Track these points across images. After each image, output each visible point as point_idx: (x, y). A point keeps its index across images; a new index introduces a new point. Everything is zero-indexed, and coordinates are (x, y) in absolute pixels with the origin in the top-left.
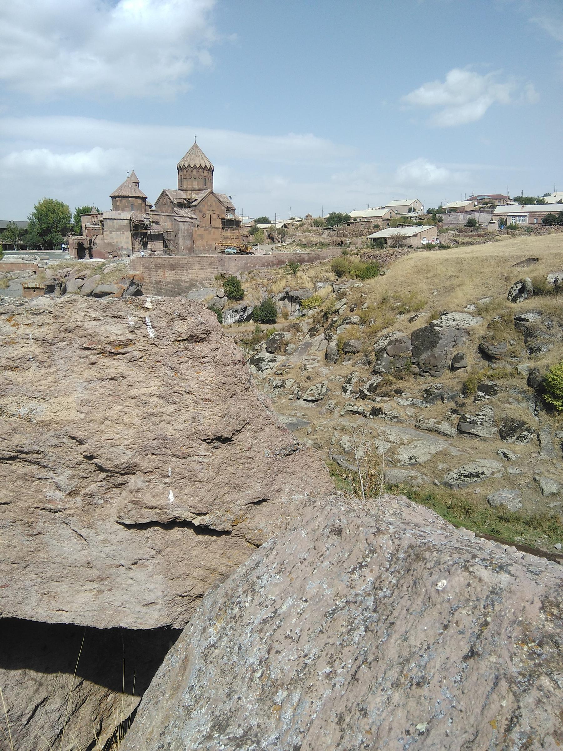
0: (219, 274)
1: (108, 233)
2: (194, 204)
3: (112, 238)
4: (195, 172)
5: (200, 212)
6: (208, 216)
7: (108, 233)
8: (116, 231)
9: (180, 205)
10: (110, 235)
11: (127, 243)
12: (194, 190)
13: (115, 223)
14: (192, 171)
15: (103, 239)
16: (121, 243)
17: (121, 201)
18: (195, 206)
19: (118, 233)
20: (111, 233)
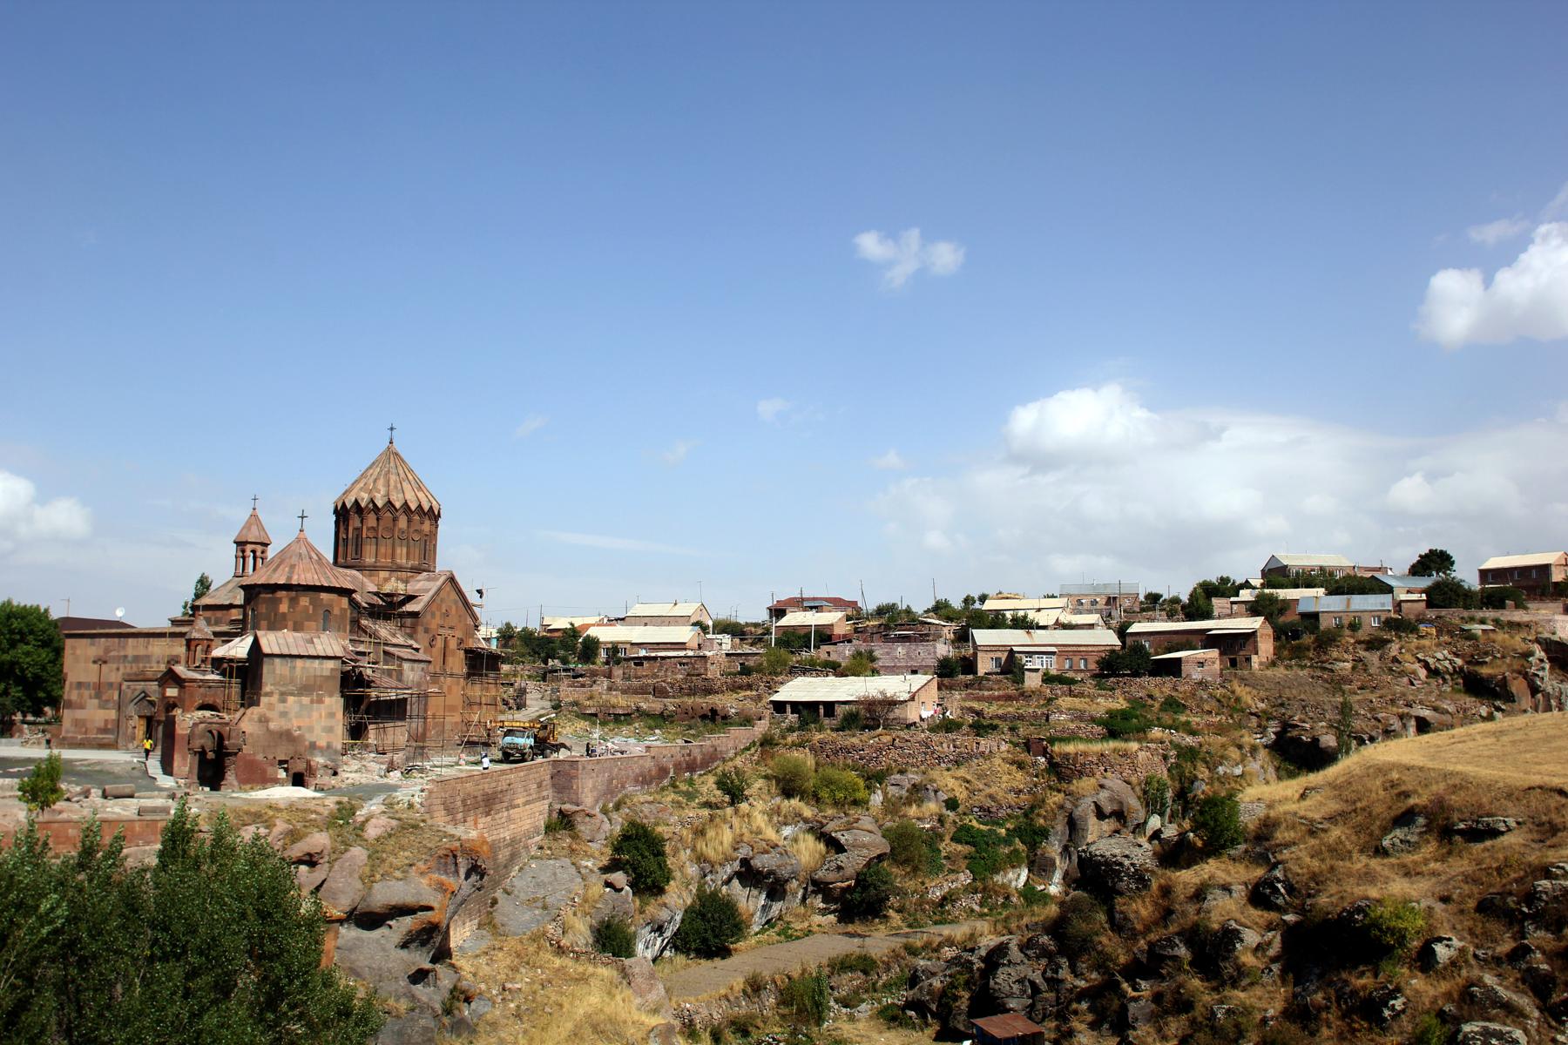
0: (555, 815)
1: (275, 699)
2: (409, 607)
3: (284, 714)
4: (402, 522)
5: (427, 631)
6: (439, 643)
7: (275, 699)
8: (300, 695)
9: (375, 613)
10: (281, 707)
11: (330, 730)
12: (400, 569)
13: (298, 671)
14: (395, 520)
15: (264, 720)
16: (311, 729)
17: (293, 602)
18: (415, 615)
19: (306, 700)
20: (284, 701)
